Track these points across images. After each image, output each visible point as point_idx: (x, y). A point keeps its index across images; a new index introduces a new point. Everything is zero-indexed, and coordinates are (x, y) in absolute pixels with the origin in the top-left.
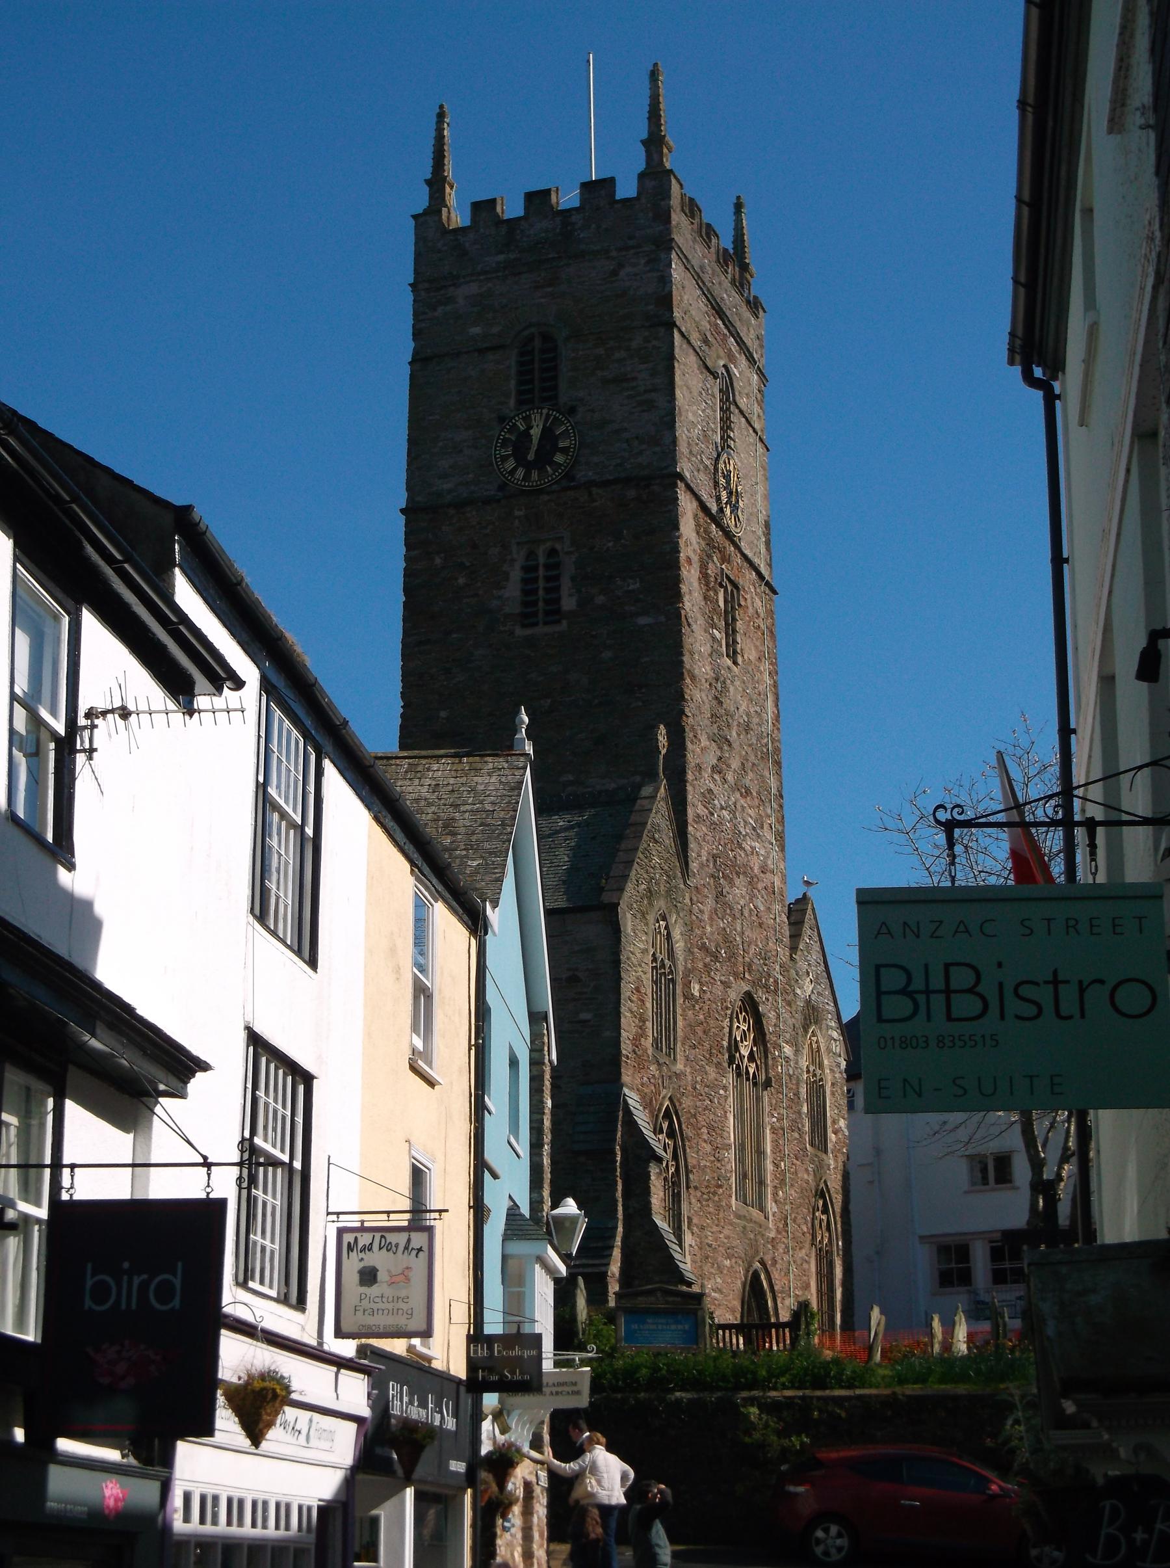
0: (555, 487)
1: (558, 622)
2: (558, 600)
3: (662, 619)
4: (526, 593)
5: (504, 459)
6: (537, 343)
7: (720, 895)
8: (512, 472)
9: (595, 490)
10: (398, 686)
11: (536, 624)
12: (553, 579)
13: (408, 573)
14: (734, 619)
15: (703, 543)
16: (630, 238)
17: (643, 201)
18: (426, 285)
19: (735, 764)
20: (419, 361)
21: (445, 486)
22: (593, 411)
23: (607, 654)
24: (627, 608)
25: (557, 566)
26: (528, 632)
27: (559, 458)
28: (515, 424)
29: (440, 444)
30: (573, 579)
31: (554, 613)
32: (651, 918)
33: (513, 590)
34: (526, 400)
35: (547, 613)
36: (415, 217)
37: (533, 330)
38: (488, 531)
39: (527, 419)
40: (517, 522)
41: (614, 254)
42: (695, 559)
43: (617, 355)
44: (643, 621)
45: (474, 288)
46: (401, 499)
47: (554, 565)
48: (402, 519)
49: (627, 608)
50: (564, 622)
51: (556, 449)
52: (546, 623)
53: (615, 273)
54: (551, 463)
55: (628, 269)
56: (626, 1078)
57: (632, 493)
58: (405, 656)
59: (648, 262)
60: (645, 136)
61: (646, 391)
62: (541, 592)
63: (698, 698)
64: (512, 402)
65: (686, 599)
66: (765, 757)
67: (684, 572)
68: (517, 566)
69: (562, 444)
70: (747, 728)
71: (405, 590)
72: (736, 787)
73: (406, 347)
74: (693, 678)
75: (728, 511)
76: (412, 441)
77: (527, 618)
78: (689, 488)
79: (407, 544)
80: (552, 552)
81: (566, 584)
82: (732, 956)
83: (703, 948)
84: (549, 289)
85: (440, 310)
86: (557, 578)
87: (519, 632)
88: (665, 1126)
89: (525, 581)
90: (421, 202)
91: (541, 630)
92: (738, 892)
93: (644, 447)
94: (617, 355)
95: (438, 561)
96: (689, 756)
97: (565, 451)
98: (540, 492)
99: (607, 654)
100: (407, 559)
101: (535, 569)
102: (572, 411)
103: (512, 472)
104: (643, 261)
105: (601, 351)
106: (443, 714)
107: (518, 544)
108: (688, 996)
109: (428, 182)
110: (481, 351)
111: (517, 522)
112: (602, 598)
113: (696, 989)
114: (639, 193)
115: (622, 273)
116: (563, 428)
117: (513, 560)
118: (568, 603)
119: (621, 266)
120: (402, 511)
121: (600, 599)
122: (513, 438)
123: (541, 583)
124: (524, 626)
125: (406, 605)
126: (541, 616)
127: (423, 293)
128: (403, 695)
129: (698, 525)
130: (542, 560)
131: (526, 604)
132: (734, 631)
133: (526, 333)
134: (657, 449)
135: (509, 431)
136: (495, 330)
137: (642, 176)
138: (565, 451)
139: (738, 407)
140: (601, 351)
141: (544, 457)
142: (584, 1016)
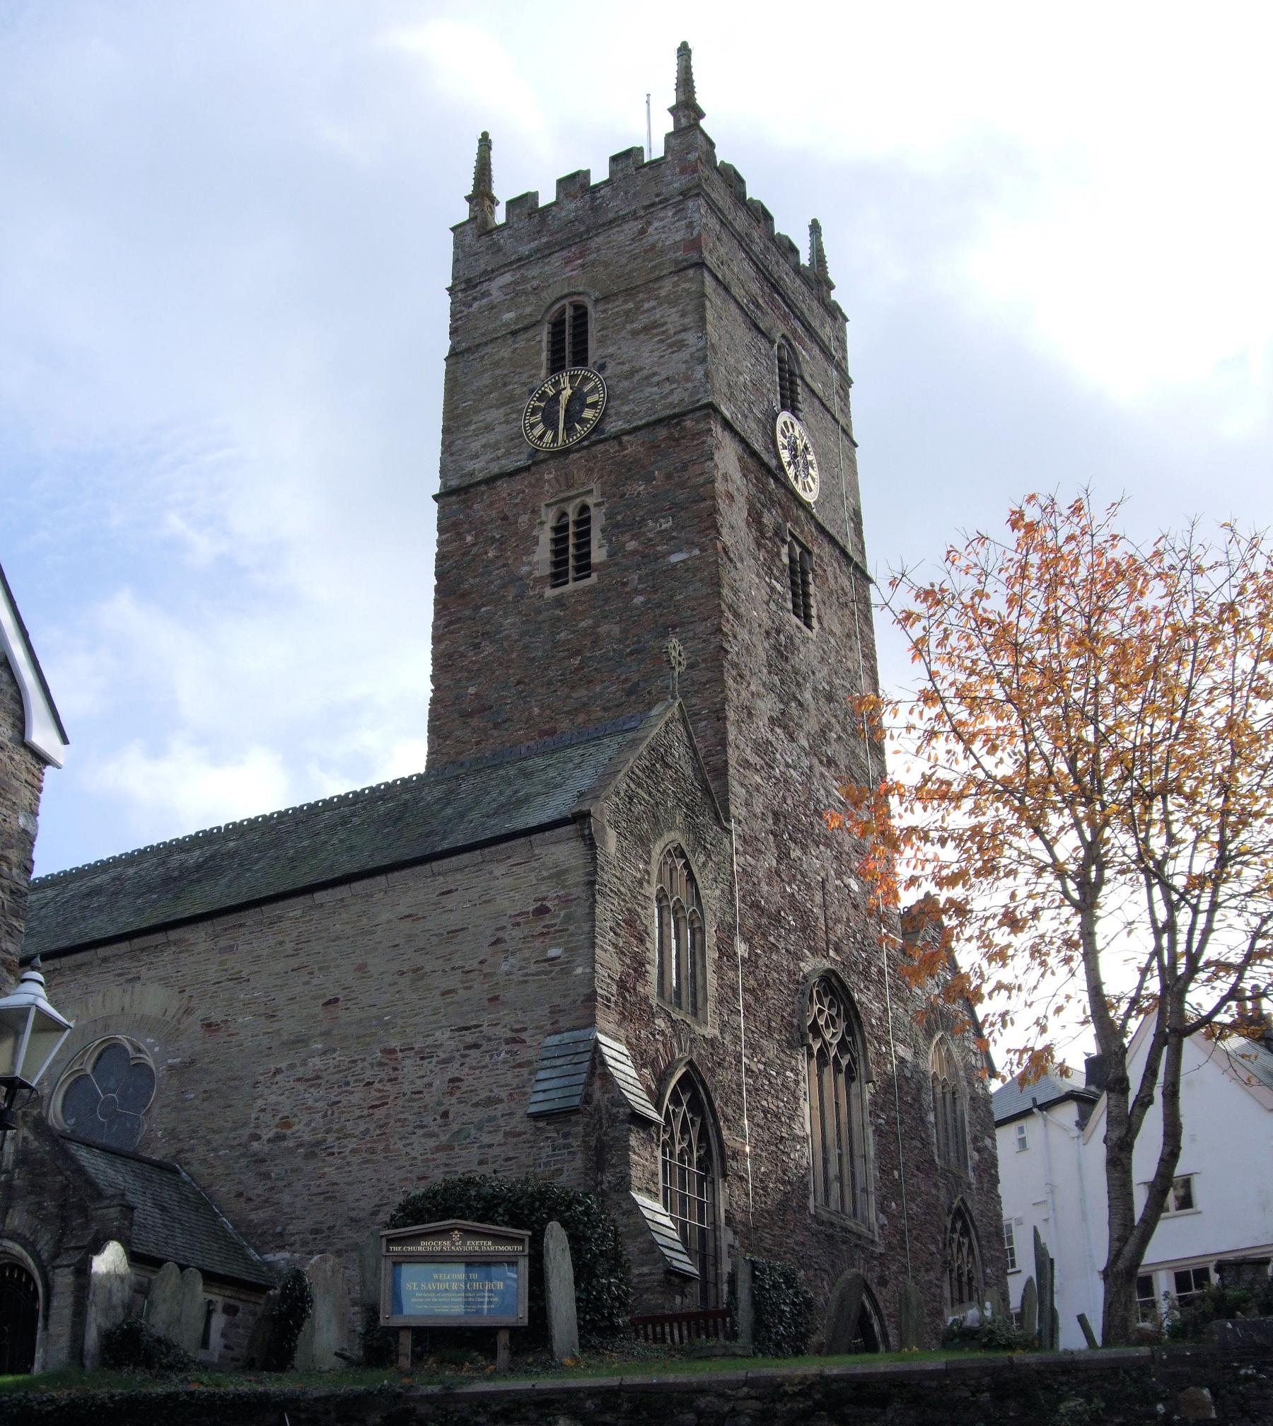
0: (585, 443)
1: (589, 576)
2: (589, 554)
3: (696, 552)
4: (556, 553)
5: (533, 426)
6: (569, 313)
7: (783, 855)
8: (541, 437)
9: (625, 438)
10: (429, 670)
11: (567, 582)
12: (584, 537)
13: (440, 558)
14: (805, 583)
15: (753, 490)
16: (657, 195)
17: (669, 158)
18: (463, 286)
19: (811, 725)
20: (454, 356)
21: (477, 466)
22: (623, 363)
23: (639, 599)
24: (659, 548)
25: (588, 520)
26: (558, 591)
27: (588, 414)
28: (544, 392)
29: (473, 427)
30: (603, 531)
31: (584, 567)
32: (657, 849)
33: (543, 554)
34: (556, 365)
35: (578, 569)
36: (453, 229)
37: (565, 302)
38: (518, 501)
39: (556, 384)
40: (547, 487)
41: (642, 213)
42: (741, 502)
43: (647, 306)
44: (675, 558)
45: (507, 278)
46: (436, 486)
47: (584, 521)
48: (435, 506)
49: (659, 548)
50: (594, 576)
51: (585, 406)
52: (576, 580)
53: (643, 232)
54: (583, 421)
55: (656, 224)
56: (600, 1022)
57: (662, 433)
58: (436, 639)
59: (675, 214)
60: (672, 102)
61: (675, 333)
62: (571, 550)
63: (748, 643)
64: (543, 372)
65: (724, 531)
66: (856, 734)
67: (722, 505)
68: (547, 527)
69: (590, 400)
70: (830, 698)
71: (436, 574)
72: (813, 751)
73: (445, 345)
74: (737, 615)
75: (791, 472)
76: (446, 431)
77: (558, 577)
78: (727, 425)
79: (441, 530)
80: (584, 509)
81: (596, 536)
82: (806, 927)
83: (755, 906)
84: (580, 261)
85: (475, 305)
86: (587, 533)
87: (550, 593)
88: (685, 1099)
89: (555, 541)
90: (462, 213)
91: (571, 586)
92: (817, 861)
93: (675, 386)
94: (647, 306)
95: (469, 539)
96: (732, 695)
97: (594, 405)
98: (566, 452)
99: (639, 599)
100: (440, 543)
101: (566, 527)
102: (602, 368)
103: (541, 437)
104: (670, 214)
105: (631, 305)
106: (472, 690)
107: (547, 505)
108: (726, 953)
109: (469, 199)
110: (514, 333)
111: (547, 487)
112: (633, 543)
113: (741, 949)
114: (666, 152)
115: (651, 230)
116: (592, 384)
117: (542, 523)
118: (598, 554)
119: (649, 223)
120: (436, 498)
121: (632, 545)
122: (542, 405)
123: (572, 541)
124: (554, 586)
125: (438, 590)
126: (571, 574)
127: (460, 295)
128: (434, 678)
129: (740, 459)
130: (572, 517)
131: (556, 564)
132: (806, 595)
133: (557, 306)
134: (690, 385)
135: (539, 400)
136: (528, 310)
137: (668, 136)
138: (594, 405)
139: (802, 378)
140: (631, 305)
141: (573, 417)
142: (553, 952)
